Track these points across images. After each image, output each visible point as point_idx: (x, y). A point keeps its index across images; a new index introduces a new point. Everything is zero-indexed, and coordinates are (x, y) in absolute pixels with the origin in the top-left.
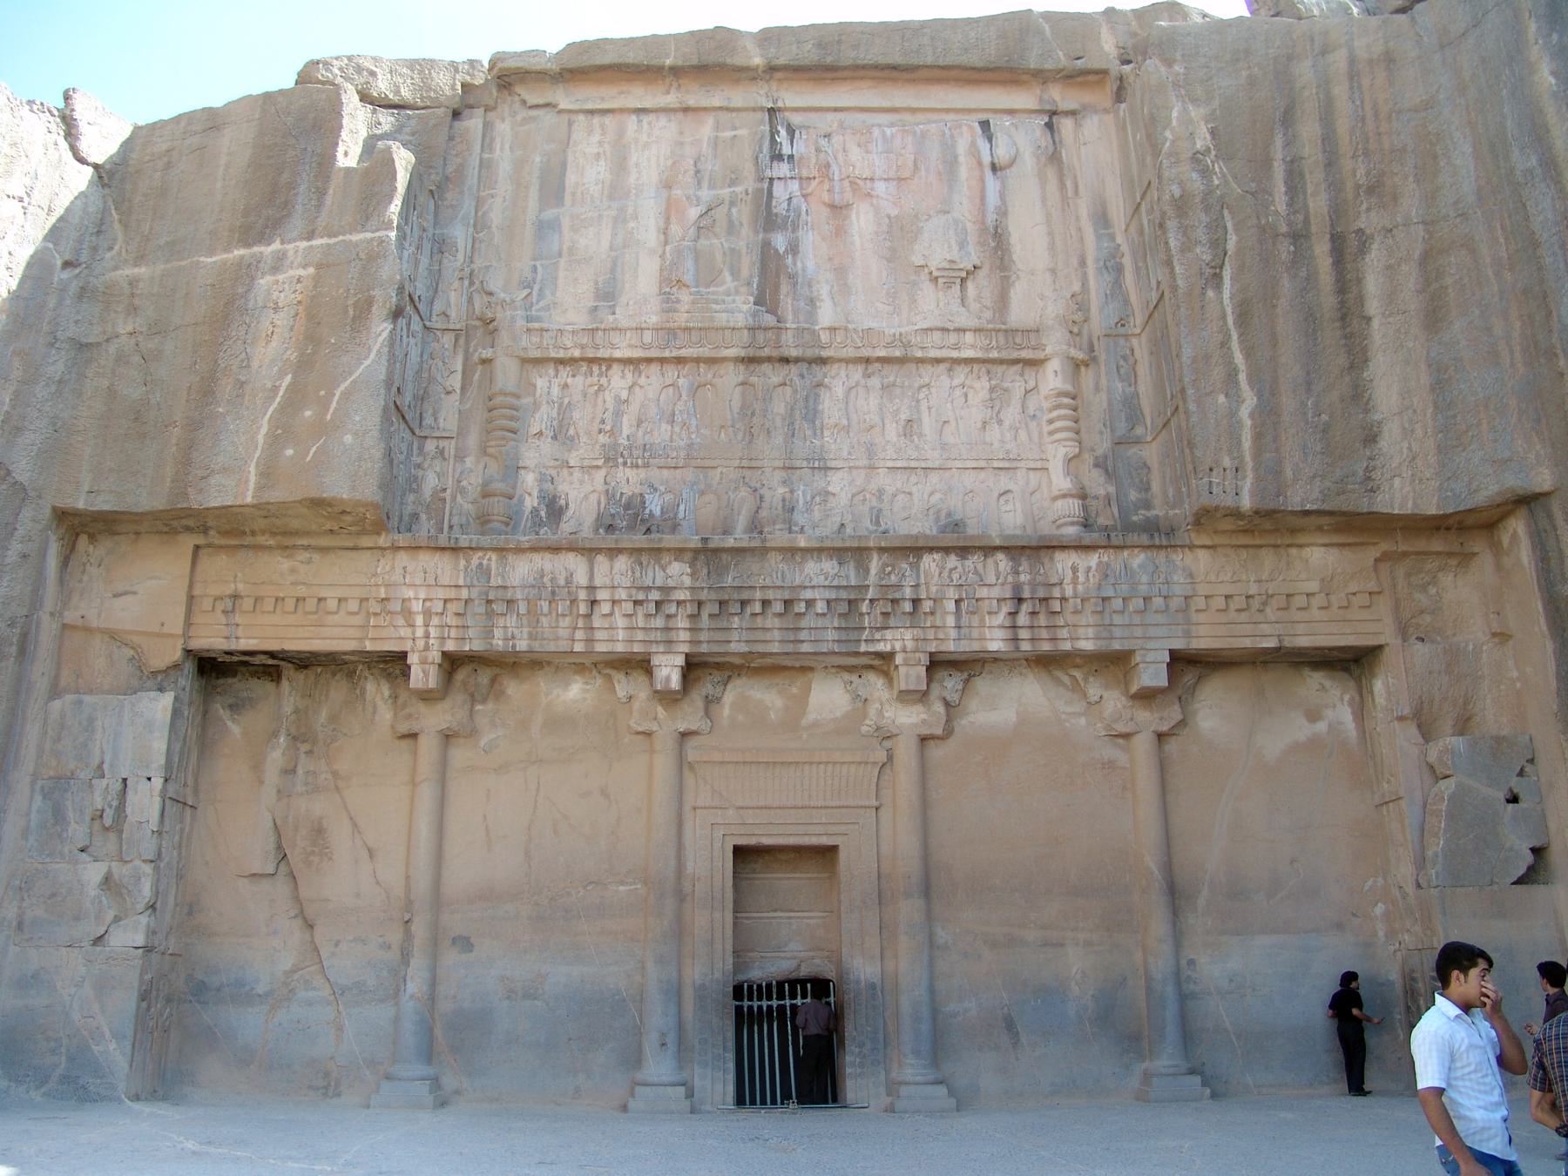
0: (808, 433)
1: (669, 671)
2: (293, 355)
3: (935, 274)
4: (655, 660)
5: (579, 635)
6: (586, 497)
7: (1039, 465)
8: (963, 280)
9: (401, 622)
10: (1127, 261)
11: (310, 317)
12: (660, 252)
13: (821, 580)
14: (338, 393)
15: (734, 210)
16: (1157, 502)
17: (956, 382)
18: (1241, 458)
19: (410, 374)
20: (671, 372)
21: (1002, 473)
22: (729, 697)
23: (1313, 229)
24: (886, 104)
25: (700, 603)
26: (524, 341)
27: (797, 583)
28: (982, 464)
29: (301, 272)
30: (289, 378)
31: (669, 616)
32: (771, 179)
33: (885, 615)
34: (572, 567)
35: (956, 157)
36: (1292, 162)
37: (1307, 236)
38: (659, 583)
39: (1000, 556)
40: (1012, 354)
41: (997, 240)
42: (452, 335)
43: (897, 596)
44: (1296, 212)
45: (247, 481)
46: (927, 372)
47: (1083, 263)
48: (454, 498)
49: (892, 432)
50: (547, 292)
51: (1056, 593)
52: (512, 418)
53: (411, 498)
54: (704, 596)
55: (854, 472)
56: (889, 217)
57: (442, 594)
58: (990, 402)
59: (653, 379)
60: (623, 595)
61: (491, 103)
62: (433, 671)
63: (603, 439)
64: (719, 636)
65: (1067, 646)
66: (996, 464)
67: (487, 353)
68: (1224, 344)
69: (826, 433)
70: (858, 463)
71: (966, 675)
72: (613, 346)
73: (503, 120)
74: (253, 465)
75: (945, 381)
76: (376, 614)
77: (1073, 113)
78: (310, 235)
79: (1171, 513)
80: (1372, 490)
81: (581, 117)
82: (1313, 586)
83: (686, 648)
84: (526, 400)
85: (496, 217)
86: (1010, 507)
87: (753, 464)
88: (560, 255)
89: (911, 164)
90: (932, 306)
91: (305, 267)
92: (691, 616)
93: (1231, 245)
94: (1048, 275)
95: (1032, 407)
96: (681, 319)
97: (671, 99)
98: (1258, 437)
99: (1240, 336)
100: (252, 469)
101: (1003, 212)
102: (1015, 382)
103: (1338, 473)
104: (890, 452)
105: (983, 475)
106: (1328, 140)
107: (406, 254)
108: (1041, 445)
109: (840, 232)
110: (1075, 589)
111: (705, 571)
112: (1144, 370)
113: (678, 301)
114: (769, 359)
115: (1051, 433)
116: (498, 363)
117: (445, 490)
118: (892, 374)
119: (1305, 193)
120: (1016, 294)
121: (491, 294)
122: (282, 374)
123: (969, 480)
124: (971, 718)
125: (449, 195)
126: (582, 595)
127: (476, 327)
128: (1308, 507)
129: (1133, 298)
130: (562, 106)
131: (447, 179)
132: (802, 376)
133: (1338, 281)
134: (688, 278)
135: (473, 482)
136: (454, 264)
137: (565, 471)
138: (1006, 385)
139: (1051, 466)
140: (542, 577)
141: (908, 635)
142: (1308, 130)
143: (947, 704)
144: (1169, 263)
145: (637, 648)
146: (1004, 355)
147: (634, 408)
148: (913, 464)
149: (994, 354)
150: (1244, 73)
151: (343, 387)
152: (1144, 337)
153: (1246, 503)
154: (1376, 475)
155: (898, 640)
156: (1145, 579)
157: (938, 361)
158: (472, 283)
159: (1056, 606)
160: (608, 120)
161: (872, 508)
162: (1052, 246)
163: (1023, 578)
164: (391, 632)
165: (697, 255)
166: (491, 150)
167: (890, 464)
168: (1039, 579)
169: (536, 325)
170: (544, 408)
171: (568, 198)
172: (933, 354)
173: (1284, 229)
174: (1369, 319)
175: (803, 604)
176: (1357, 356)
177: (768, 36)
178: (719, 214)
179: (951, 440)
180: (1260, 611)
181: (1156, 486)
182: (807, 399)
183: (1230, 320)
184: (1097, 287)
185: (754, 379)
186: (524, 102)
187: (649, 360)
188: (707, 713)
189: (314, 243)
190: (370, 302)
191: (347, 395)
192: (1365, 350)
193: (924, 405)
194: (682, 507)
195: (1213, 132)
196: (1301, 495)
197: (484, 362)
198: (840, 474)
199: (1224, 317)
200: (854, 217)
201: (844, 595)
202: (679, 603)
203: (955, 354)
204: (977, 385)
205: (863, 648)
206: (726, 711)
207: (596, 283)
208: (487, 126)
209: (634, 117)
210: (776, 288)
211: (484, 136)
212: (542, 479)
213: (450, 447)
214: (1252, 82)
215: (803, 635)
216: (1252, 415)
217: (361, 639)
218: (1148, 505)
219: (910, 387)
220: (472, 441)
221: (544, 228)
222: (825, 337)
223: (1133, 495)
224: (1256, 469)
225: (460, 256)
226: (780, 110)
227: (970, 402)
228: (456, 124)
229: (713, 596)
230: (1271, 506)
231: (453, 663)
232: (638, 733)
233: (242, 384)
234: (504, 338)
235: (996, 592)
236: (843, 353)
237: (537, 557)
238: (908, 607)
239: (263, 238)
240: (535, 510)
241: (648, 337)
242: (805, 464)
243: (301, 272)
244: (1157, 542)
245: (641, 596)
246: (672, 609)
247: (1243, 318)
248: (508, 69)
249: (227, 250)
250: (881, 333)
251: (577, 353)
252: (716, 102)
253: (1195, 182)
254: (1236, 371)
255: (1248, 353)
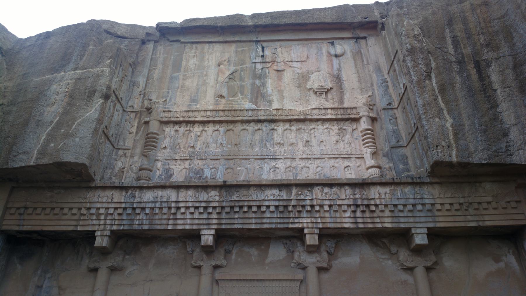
0: (268, 146)
1: (208, 237)
2: (61, 110)
3: (316, 90)
4: (202, 232)
5: (171, 222)
6: (181, 170)
7: (360, 156)
8: (326, 93)
9: (94, 217)
10: (390, 84)
11: (70, 97)
12: (215, 86)
13: (271, 198)
14: (76, 123)
15: (242, 73)
16: (412, 169)
17: (325, 127)
18: (450, 142)
19: (113, 124)
20: (217, 127)
21: (345, 159)
22: (234, 251)
23: (466, 59)
24: (297, 38)
25: (223, 208)
26: (162, 115)
27: (262, 198)
28: (337, 156)
29: (70, 81)
30: (57, 119)
31: (210, 213)
32: (255, 63)
33: (299, 212)
34: (171, 194)
35: (322, 54)
36: (454, 37)
37: (465, 62)
38: (205, 199)
39: (347, 187)
40: (346, 118)
41: (338, 79)
42: (134, 114)
43: (304, 203)
44: (458, 54)
45: (32, 157)
46: (314, 125)
47: (372, 85)
48: (128, 172)
49: (300, 146)
50: (173, 100)
51: (372, 202)
52: (154, 142)
53: (109, 171)
54: (224, 204)
55: (286, 160)
56: (298, 73)
57: (113, 205)
58: (338, 134)
59: (210, 128)
60: (190, 204)
61: (157, 39)
62: (106, 239)
63: (189, 149)
64: (229, 221)
65: (379, 226)
66: (342, 156)
67: (147, 119)
68: (436, 100)
69: (275, 146)
70: (287, 157)
71: (335, 241)
72: (195, 117)
73: (161, 45)
74: (36, 150)
75: (320, 127)
76: (84, 215)
77: (365, 38)
78: (76, 69)
79: (419, 171)
80: (510, 155)
81: (189, 45)
82: (489, 199)
83: (215, 227)
84: (161, 136)
85: (156, 74)
86: (350, 172)
87: (247, 157)
88: (178, 88)
89: (306, 56)
90: (315, 102)
91: (71, 80)
92: (218, 213)
93: (433, 65)
94: (359, 91)
95: (355, 136)
96: (221, 107)
97: (221, 39)
98: (456, 134)
99: (442, 97)
100: (36, 152)
101: (339, 70)
102: (349, 127)
103: (494, 148)
104: (301, 153)
105: (337, 160)
106: (467, 30)
107: (114, 80)
108: (360, 149)
109: (280, 79)
110: (380, 201)
111: (225, 194)
112: (400, 121)
113: (220, 101)
114: (254, 121)
115: (364, 144)
116: (151, 123)
117: (124, 168)
118: (301, 125)
119: (461, 48)
120: (347, 97)
121: (151, 100)
122: (55, 116)
123: (332, 162)
124: (340, 260)
125: (138, 68)
126: (173, 205)
127: (144, 111)
128: (483, 162)
129: (393, 96)
130: (182, 41)
131: (138, 63)
132: (266, 126)
133: (479, 77)
134: (224, 94)
135: (138, 165)
136: (137, 91)
137: (174, 161)
138: (344, 128)
139: (365, 156)
140: (157, 198)
141: (309, 220)
142: (458, 27)
143: (329, 253)
144: (409, 73)
145: (195, 227)
146: (343, 117)
147: (203, 138)
148: (309, 157)
149: (340, 117)
150: (431, 10)
151: (78, 121)
152: (399, 108)
153: (455, 159)
154: (511, 148)
155: (304, 222)
156: (411, 197)
157: (317, 120)
158: (144, 97)
159: (373, 208)
160: (199, 46)
161: (293, 173)
162: (360, 81)
163: (357, 196)
164: (91, 223)
165: (228, 87)
166: (156, 55)
167: (300, 157)
168: (364, 197)
169: (167, 110)
170: (168, 139)
171: (182, 70)
172: (315, 117)
173: (454, 60)
174: (495, 90)
175: (265, 207)
176: (494, 105)
177: (254, 16)
178: (237, 74)
179: (324, 148)
180: (466, 210)
181: (410, 162)
182: (268, 134)
183: (437, 91)
184: (378, 93)
185: (248, 128)
186: (168, 40)
187: (209, 122)
188: (225, 258)
189: (76, 72)
190: (95, 91)
191: (79, 125)
192: (496, 101)
193: (313, 136)
194: (219, 173)
195: (420, 28)
196: (479, 157)
197: (147, 123)
198: (280, 161)
199: (434, 90)
200: (285, 74)
201: (281, 203)
202: (215, 208)
203: (324, 117)
204: (333, 128)
205: (291, 226)
206: (234, 257)
207: (191, 97)
208: (155, 47)
209: (207, 45)
210: (257, 98)
211: (153, 50)
212: (163, 165)
213: (128, 153)
214: (434, 13)
215: (265, 221)
216: (452, 126)
217: (76, 226)
218: (408, 171)
219: (307, 129)
220: (138, 150)
221: (172, 79)
222: (275, 112)
223: (401, 166)
224: (457, 147)
225: (141, 88)
226: (259, 41)
227: (331, 134)
228: (144, 46)
229: (228, 204)
230: (467, 161)
231: (117, 237)
232: (195, 267)
233: (39, 121)
234: (154, 113)
235: (346, 202)
236: (281, 118)
237: (156, 190)
238: (309, 208)
239: (57, 71)
240: (160, 175)
241: (208, 113)
242: (267, 157)
243: (70, 81)
244: (415, 181)
245: (197, 205)
246: (210, 210)
247: (443, 90)
248: (163, 27)
249: (44, 76)
250: (295, 110)
251: (182, 119)
252: (236, 39)
253: (416, 43)
254: (442, 110)
255: (446, 103)
